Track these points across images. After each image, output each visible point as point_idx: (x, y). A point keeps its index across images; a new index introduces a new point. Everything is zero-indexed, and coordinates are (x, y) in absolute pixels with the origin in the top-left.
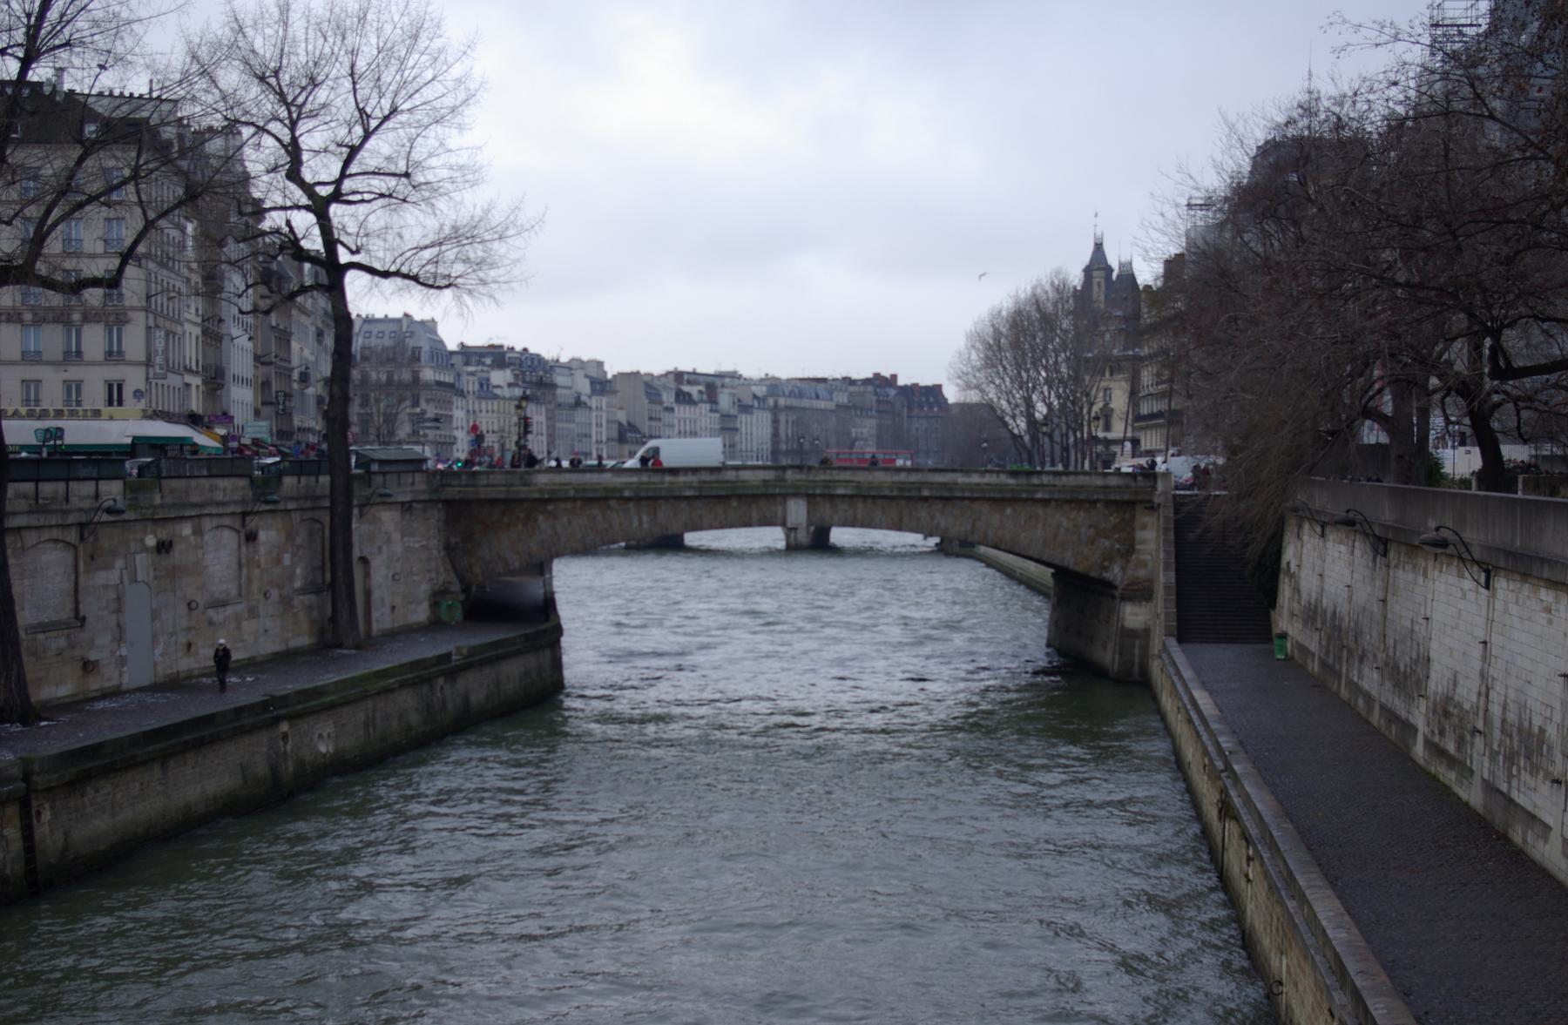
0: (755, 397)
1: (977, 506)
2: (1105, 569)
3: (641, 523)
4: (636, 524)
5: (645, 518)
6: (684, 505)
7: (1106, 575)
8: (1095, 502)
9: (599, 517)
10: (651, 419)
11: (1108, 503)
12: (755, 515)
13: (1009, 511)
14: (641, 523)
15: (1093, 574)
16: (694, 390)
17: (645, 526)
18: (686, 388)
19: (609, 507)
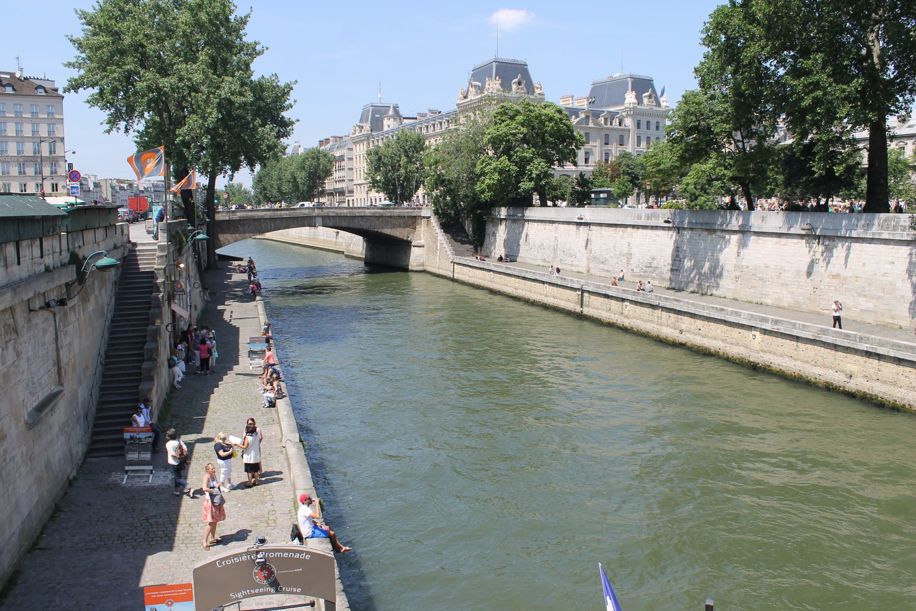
0: (144, 188)
1: (371, 218)
2: (408, 237)
4: (269, 227)
6: (284, 220)
7: (409, 239)
8: (404, 217)
9: (258, 225)
11: (409, 217)
12: (306, 223)
13: (381, 220)
15: (405, 238)
17: (273, 227)
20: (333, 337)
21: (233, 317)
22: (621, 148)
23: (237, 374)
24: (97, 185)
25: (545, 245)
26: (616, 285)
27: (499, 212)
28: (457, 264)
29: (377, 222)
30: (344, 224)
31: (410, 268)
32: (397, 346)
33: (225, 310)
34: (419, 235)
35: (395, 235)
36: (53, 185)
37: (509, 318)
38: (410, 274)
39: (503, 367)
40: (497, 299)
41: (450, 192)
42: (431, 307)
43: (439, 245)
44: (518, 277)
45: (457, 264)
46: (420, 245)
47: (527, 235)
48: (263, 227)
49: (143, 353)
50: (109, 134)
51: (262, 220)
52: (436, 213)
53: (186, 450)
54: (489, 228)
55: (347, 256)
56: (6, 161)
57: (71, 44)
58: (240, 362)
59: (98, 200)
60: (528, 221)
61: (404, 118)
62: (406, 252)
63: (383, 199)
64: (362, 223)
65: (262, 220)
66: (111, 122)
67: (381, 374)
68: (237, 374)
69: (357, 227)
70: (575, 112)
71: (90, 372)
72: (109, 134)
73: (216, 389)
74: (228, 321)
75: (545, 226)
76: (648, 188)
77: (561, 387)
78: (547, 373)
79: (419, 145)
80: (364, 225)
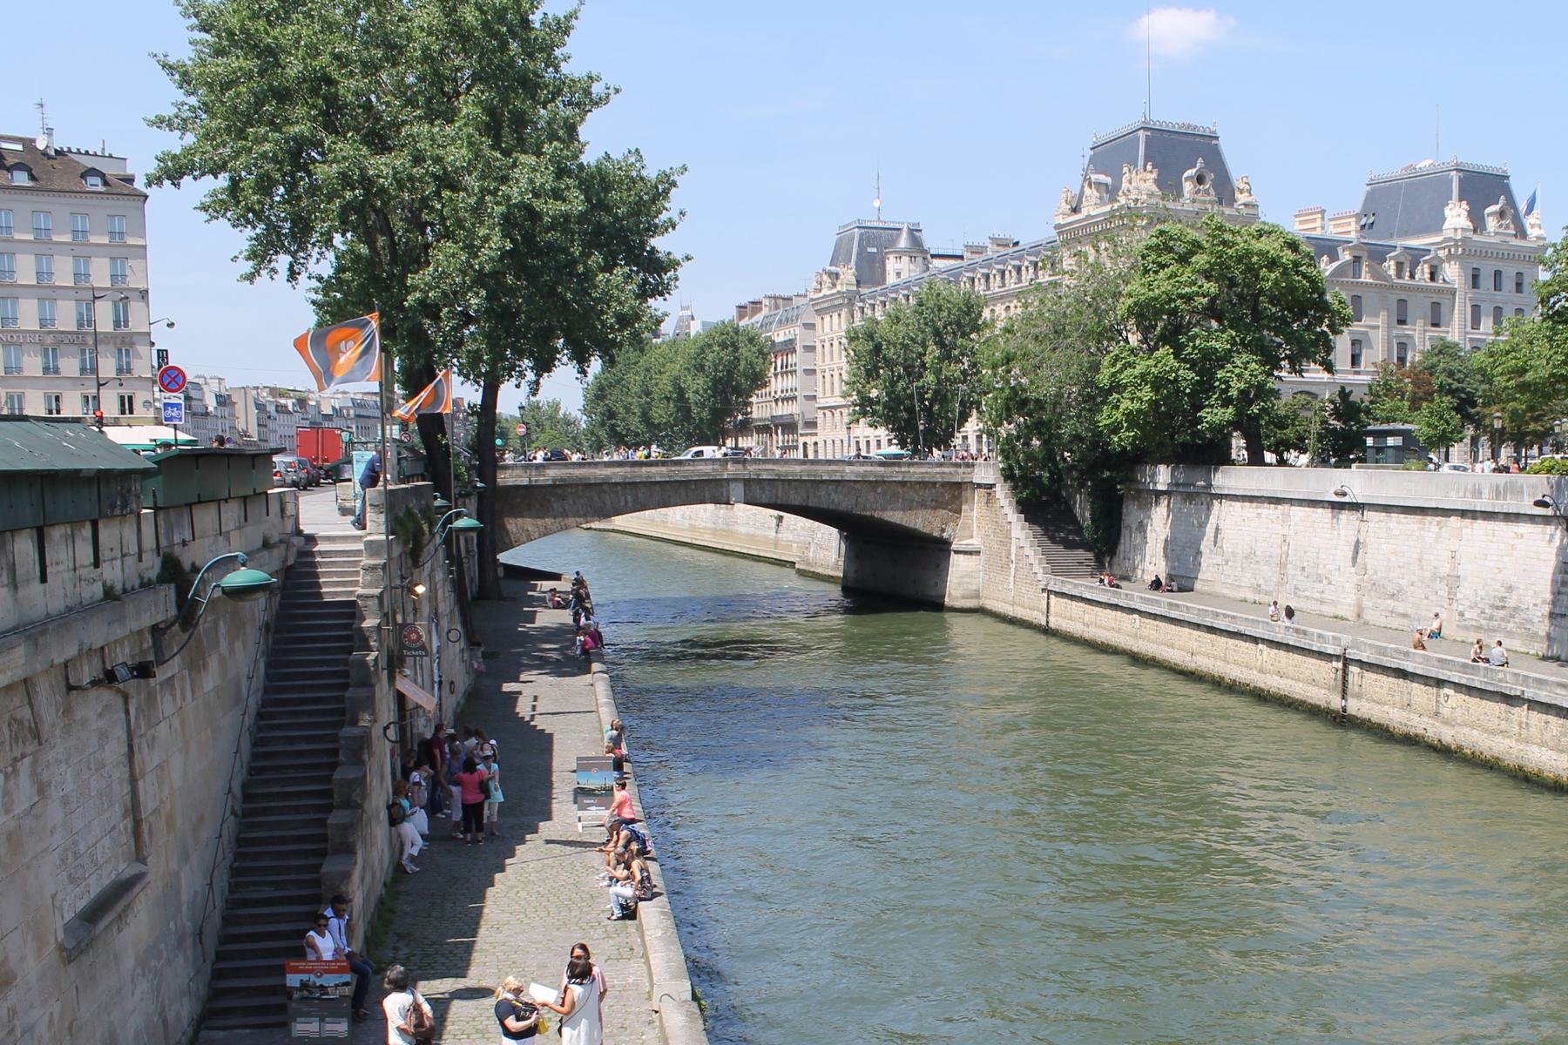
1: (858, 486)
2: (943, 530)
3: (626, 502)
4: (623, 503)
5: (629, 498)
6: (657, 488)
8: (934, 484)
9: (596, 498)
10: (259, 425)
11: (944, 484)
12: (707, 494)
13: (879, 490)
14: (626, 502)
15: (936, 534)
16: (290, 403)
17: (630, 504)
18: (283, 401)
19: (604, 491)
20: (769, 760)
21: (539, 709)
22: (1435, 332)
23: (548, 842)
24: (223, 400)
25: (1258, 553)
26: (1424, 648)
27: (1153, 476)
28: (1057, 594)
29: (871, 496)
30: (795, 499)
31: (948, 601)
32: (918, 782)
33: (520, 693)
34: (969, 527)
35: (912, 526)
36: (122, 398)
37: (1176, 721)
38: (947, 616)
39: (1162, 834)
40: (1148, 677)
41: (1039, 427)
42: (995, 692)
43: (1013, 551)
44: (1197, 626)
45: (1057, 594)
46: (969, 548)
47: (1217, 529)
48: (608, 502)
49: (331, 790)
50: (252, 283)
51: (605, 487)
52: (1008, 475)
53: (430, 1014)
54: (1131, 513)
55: (802, 573)
56: (15, 342)
57: (163, 74)
58: (555, 814)
59: (227, 436)
60: (1221, 497)
61: (933, 256)
62: (938, 566)
63: (884, 443)
64: (836, 498)
65: (605, 487)
66: (256, 257)
67: (881, 846)
68: (548, 842)
69: (825, 506)
70: (1329, 248)
71: (207, 833)
72: (252, 283)
73: (498, 876)
74: (527, 719)
75: (1259, 511)
76: (1497, 424)
77: (1297, 883)
78: (1264, 850)
79: (967, 318)
80: (842, 502)
